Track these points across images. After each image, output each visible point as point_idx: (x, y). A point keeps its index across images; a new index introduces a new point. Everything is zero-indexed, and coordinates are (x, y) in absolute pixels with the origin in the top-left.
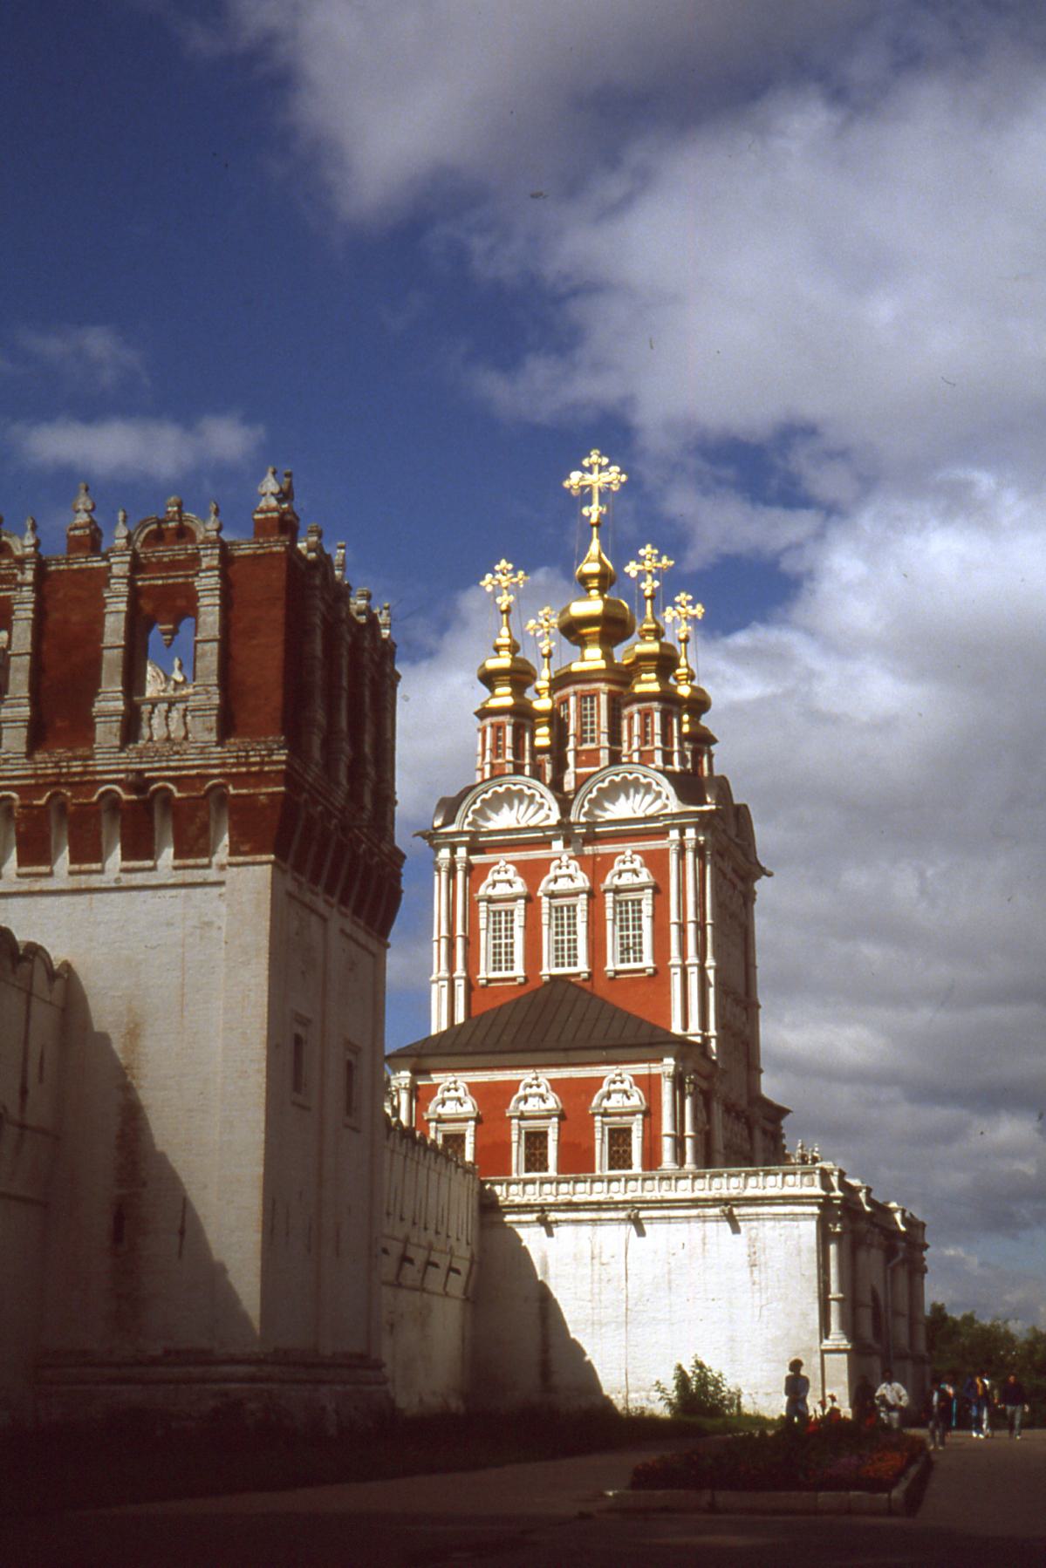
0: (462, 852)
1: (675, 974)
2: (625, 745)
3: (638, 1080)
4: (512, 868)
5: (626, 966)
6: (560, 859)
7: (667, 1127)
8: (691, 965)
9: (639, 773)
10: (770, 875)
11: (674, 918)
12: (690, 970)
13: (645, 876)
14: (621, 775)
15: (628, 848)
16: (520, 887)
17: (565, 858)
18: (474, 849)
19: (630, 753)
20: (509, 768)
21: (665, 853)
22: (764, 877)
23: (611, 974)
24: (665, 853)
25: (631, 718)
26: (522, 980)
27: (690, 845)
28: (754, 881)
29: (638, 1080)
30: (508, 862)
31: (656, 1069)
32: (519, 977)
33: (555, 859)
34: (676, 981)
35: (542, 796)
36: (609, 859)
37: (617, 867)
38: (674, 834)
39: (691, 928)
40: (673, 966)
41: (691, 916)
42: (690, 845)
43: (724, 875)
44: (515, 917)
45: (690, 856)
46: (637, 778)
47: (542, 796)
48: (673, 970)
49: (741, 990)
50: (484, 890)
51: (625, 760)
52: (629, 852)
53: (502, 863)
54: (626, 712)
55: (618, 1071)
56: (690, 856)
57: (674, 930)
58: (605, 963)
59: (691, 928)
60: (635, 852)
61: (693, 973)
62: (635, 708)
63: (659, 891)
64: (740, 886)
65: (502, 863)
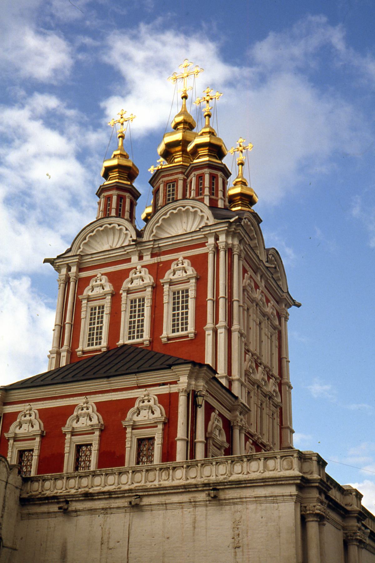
0: (74, 269)
1: (209, 335)
3: (161, 399)
4: (104, 278)
5: (176, 334)
6: (136, 268)
7: (181, 432)
8: (220, 327)
9: (189, 203)
10: (299, 306)
11: (210, 296)
12: (219, 331)
13: (191, 271)
14: (178, 209)
15: (180, 256)
16: (109, 288)
18: (80, 270)
23: (164, 340)
26: (104, 350)
27: (221, 245)
29: (161, 399)
30: (102, 275)
31: (174, 389)
33: (132, 269)
34: (209, 340)
35: (127, 229)
36: (167, 265)
37: (173, 266)
38: (211, 240)
39: (222, 302)
40: (208, 329)
41: (222, 293)
42: (221, 245)
45: (222, 254)
48: (207, 333)
50: (87, 292)
52: (181, 259)
53: (99, 275)
55: (146, 393)
56: (222, 254)
57: (210, 305)
58: (162, 333)
59: (222, 302)
60: (185, 258)
63: (201, 280)
65: (99, 275)
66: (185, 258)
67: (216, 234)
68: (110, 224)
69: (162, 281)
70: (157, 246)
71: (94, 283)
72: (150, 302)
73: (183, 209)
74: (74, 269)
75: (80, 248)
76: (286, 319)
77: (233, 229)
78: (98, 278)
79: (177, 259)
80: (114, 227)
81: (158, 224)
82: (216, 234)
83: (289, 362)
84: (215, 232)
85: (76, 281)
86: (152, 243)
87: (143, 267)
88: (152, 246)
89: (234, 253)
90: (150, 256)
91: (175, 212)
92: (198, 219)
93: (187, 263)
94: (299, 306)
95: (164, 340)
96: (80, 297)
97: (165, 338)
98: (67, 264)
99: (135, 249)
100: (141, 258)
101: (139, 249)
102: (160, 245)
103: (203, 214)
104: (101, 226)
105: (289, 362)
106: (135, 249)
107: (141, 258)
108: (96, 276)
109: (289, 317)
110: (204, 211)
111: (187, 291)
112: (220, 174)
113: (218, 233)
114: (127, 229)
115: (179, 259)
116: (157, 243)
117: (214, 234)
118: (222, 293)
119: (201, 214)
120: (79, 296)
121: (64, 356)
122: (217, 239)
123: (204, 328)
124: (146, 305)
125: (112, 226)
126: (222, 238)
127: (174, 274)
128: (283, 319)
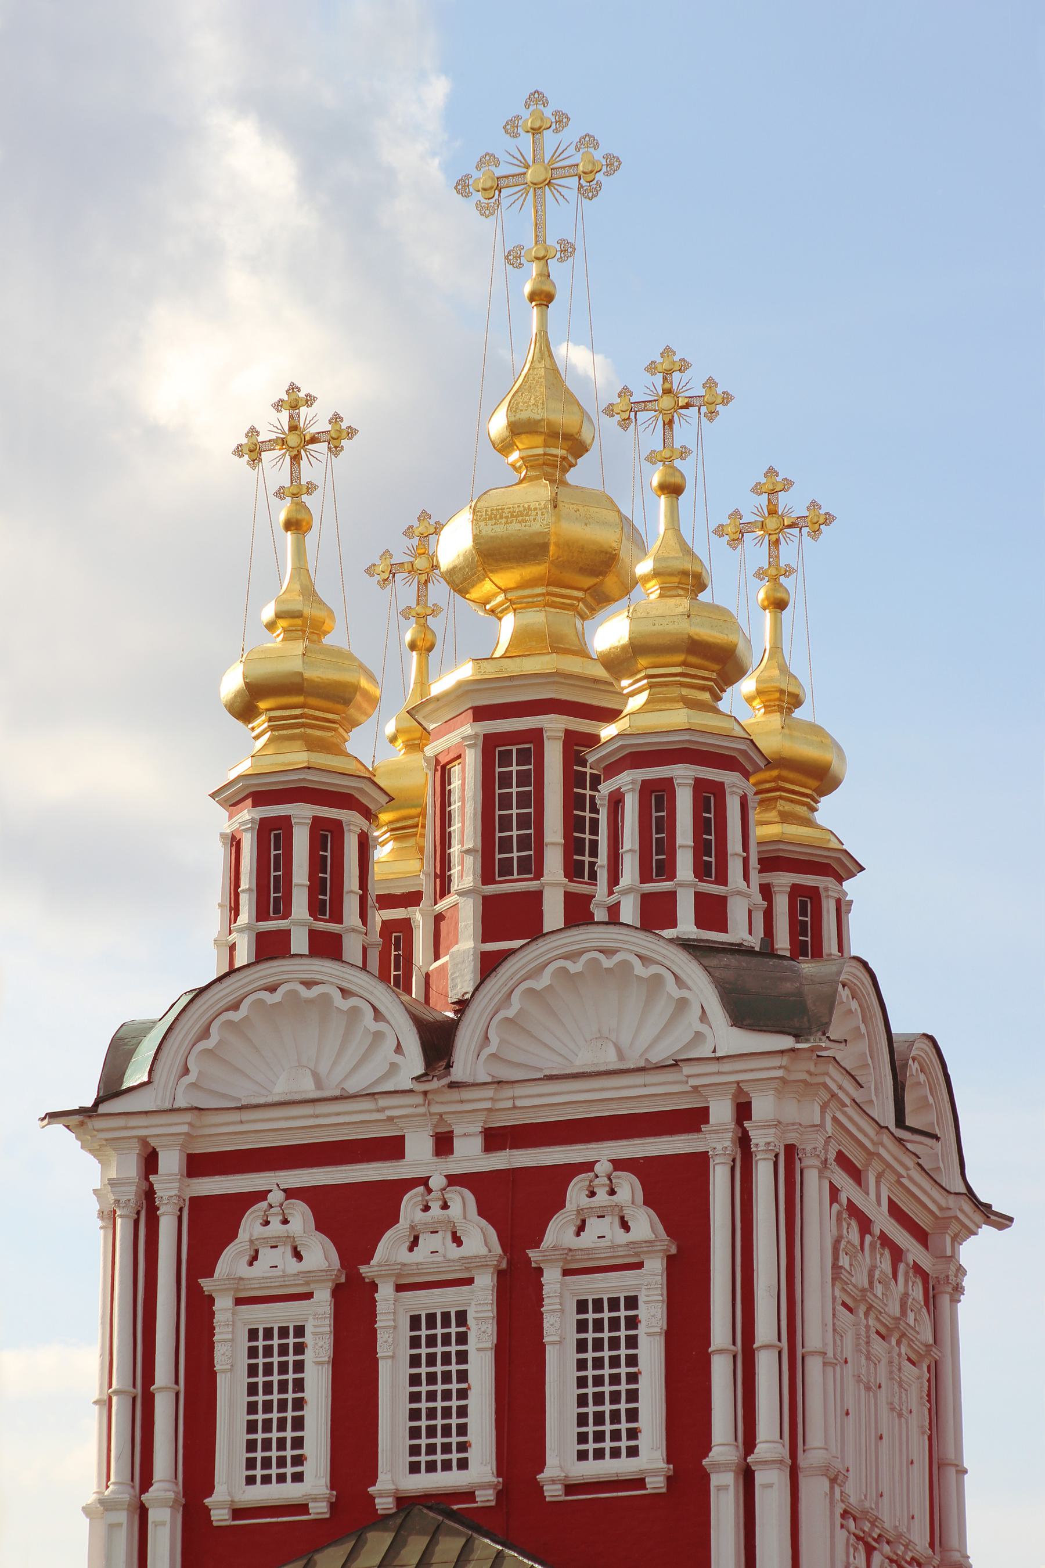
0: (171, 1162)
2: (603, 876)
6: (424, 1181)
10: (1003, 1221)
12: (760, 1478)
14: (586, 957)
17: (437, 1182)
19: (612, 900)
20: (299, 943)
21: (700, 1162)
22: (986, 1231)
23: (553, 1492)
24: (700, 1162)
25: (616, 801)
26: (319, 1509)
28: (957, 1239)
30: (291, 1193)
32: (315, 1500)
35: (378, 1015)
37: (576, 1194)
38: (721, 1112)
40: (718, 1467)
42: (758, 1138)
43: (865, 1224)
44: (308, 1339)
46: (625, 965)
47: (378, 1015)
48: (715, 1480)
49: (919, 1537)
51: (600, 915)
52: (603, 1168)
53: (276, 1197)
54: (606, 788)
61: (770, 1486)
62: (628, 781)
64: (914, 1252)
65: (276, 1197)
66: (619, 1165)
67: (740, 1091)
68: (308, 984)
69: (532, 1254)
70: (509, 1104)
71: (259, 1231)
72: (489, 1331)
73: (607, 963)
74: (171, 1162)
75: (186, 1071)
76: (958, 1289)
77: (804, 1076)
78: (271, 1206)
79: (588, 1167)
80: (325, 998)
81: (510, 1013)
82: (740, 1091)
83: (965, 1472)
84: (738, 1083)
85: (181, 1210)
86: (489, 1093)
87: (453, 1180)
88: (488, 1105)
89: (807, 1162)
90: (478, 1142)
91: (574, 967)
92: (661, 1010)
93: (629, 1188)
94: (1003, 1221)
95: (553, 1492)
96: (206, 1284)
97: (553, 1482)
98: (144, 1141)
99: (422, 1110)
100: (444, 1144)
101: (436, 1109)
102: (519, 1103)
103: (684, 993)
104: (272, 989)
105: (965, 1472)
106: (422, 1110)
107: (444, 1144)
108: (262, 1195)
109: (966, 1282)
110: (690, 983)
111: (632, 1302)
112: (729, 778)
113: (745, 1088)
114: (399, 1049)
115: (597, 1168)
116: (508, 1092)
117: (733, 1089)
118: (765, 1329)
119: (677, 993)
120: (202, 1282)
121: (163, 1524)
122: (743, 1111)
123: (705, 1462)
124: (472, 1337)
125: (316, 991)
126: (762, 1107)
127: (581, 1229)
128: (946, 1298)
